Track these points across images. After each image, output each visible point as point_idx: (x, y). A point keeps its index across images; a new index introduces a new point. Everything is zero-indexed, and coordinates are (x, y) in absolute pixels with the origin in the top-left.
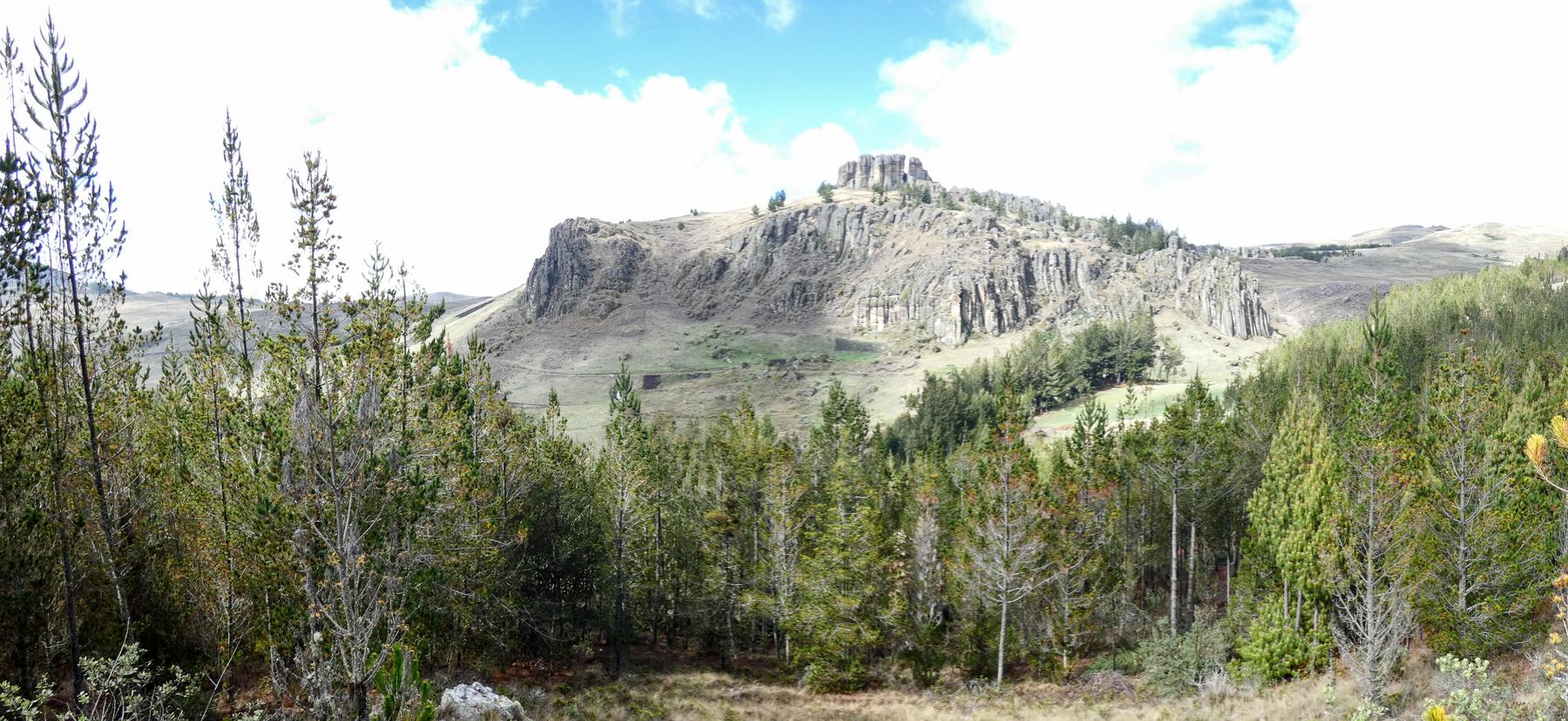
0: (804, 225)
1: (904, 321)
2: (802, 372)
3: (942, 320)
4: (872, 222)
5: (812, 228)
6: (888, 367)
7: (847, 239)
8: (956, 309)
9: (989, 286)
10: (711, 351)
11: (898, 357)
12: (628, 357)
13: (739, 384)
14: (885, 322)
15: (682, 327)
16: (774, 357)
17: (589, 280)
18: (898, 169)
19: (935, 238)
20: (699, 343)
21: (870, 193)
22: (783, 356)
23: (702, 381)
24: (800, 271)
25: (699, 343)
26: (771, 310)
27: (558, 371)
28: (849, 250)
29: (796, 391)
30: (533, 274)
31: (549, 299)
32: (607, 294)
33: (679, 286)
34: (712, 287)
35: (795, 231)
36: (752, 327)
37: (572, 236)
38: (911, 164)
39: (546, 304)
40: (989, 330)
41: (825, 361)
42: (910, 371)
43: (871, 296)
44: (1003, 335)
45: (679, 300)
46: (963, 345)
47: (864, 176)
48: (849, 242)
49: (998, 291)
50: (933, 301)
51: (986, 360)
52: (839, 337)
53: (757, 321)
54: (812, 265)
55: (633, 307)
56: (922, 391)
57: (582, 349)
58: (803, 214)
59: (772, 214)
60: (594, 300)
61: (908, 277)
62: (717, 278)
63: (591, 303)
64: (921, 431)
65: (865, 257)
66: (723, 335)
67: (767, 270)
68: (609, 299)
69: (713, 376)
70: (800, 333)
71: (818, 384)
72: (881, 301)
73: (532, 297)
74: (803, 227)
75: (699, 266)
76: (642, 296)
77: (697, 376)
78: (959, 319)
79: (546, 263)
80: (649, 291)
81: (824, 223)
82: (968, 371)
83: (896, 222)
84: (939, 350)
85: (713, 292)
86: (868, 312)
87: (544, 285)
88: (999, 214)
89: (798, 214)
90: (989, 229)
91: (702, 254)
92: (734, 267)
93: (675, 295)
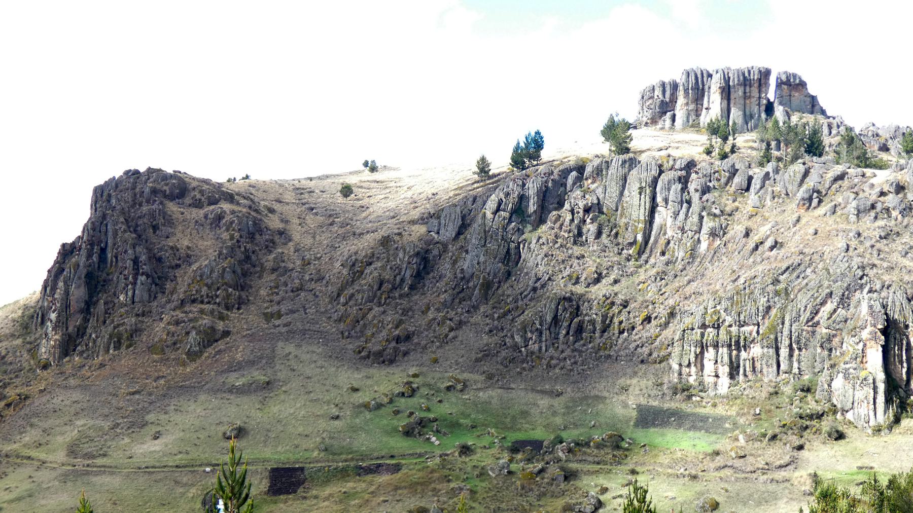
0: (578, 193)
1: (769, 374)
2: (573, 466)
3: (846, 377)
4: (706, 190)
5: (591, 199)
6: (738, 463)
7: (658, 220)
8: (875, 357)
10: (402, 422)
11: (757, 444)
12: (240, 433)
13: (452, 485)
14: (733, 375)
15: (347, 376)
16: (521, 436)
17: (169, 286)
18: (755, 93)
19: (831, 220)
20: (379, 406)
21: (703, 139)
22: (538, 434)
23: (384, 478)
25: (379, 406)
26: (516, 347)
27: (100, 461)
28: (662, 241)
30: (56, 273)
31: (86, 320)
32: (202, 312)
33: (342, 300)
34: (405, 302)
35: (561, 205)
36: (477, 378)
37: (136, 203)
38: (780, 84)
39: (81, 332)
41: (618, 447)
42: (781, 474)
43: (704, 326)
45: (342, 326)
46: (890, 428)
47: (692, 107)
48: (662, 228)
50: (829, 339)
52: (643, 401)
53: (486, 367)
54: (591, 266)
55: (252, 338)
57: (151, 417)
58: (574, 174)
59: (517, 173)
60: (177, 323)
61: (777, 293)
62: (412, 287)
63: (172, 328)
65: (693, 253)
66: (424, 391)
67: (509, 274)
68: (206, 321)
69: (404, 471)
70: (569, 392)
71: (604, 490)
73: (53, 316)
74: (576, 199)
75: (379, 264)
76: (268, 317)
77: (376, 469)
78: (881, 376)
79: (84, 252)
80: (283, 308)
81: (613, 190)
82: (903, 483)
83: (752, 189)
84: (840, 436)
85: (405, 312)
86: (700, 357)
87: (78, 293)
89: (566, 173)
91: (386, 241)
92: (445, 267)
93: (335, 316)
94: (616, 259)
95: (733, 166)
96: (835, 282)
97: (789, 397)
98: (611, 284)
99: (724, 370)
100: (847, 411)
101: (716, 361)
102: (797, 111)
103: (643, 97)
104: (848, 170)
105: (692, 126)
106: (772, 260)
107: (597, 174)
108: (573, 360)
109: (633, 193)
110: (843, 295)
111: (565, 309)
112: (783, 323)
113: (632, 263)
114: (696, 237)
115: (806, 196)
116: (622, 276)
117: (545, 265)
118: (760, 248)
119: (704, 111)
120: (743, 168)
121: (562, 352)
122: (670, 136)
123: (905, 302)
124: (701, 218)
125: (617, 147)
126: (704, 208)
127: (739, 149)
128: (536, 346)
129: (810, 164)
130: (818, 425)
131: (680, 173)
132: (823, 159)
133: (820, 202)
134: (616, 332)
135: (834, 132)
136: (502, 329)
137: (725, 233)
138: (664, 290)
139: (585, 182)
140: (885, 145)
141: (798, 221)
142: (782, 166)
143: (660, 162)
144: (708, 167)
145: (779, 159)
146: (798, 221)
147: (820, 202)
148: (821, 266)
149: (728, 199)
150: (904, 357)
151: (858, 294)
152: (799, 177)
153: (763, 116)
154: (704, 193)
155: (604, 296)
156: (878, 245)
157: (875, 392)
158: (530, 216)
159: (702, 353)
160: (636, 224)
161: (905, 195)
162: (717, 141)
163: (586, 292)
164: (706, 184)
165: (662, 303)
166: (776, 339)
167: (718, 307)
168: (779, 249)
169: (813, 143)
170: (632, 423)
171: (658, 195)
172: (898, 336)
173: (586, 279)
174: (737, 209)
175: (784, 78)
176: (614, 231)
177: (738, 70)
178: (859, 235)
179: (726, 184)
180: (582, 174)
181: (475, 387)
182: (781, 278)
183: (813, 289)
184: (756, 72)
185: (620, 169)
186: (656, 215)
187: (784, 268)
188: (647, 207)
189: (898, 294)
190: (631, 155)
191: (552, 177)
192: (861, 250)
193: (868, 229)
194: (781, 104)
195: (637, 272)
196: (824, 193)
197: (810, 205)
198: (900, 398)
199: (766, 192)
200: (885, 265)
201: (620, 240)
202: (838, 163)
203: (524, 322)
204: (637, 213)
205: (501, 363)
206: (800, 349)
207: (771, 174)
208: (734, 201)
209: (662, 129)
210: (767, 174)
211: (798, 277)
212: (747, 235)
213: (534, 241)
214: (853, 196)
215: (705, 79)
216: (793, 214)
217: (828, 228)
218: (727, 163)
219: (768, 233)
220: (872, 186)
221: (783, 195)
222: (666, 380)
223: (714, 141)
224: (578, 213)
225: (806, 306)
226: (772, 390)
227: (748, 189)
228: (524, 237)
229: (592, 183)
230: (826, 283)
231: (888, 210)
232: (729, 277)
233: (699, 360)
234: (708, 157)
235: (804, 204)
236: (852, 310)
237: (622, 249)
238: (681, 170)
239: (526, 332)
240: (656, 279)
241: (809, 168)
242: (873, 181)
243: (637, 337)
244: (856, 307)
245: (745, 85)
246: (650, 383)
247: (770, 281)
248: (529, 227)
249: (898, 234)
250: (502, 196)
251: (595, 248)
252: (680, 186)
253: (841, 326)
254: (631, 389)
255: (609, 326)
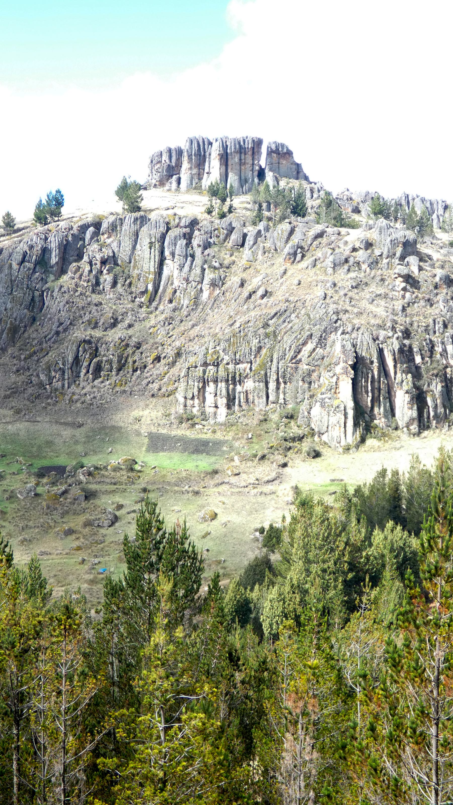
0: (95, 246)
1: (260, 404)
2: (93, 487)
3: (323, 406)
4: (207, 246)
5: (107, 252)
6: (233, 480)
7: (166, 272)
9: (401, 351)
11: (250, 464)
14: (229, 406)
16: (46, 463)
18: (249, 160)
19: (311, 272)
21: (205, 200)
22: (62, 461)
24: (89, 322)
26: (41, 385)
28: (170, 290)
29: (82, 519)
35: (80, 257)
38: (270, 152)
40: (401, 424)
44: (426, 433)
46: (357, 447)
48: (170, 279)
49: (418, 359)
50: (309, 374)
51: (395, 473)
52: (154, 430)
53: (14, 402)
56: (288, 520)
58: (92, 229)
59: (40, 228)
61: (267, 335)
64: (287, 588)
70: (90, 423)
71: (120, 507)
72: (222, 373)
78: (351, 404)
81: (127, 244)
82: (367, 492)
83: (246, 245)
84: (317, 455)
86: (202, 390)
88: (421, 233)
89: (84, 228)
90: (402, 258)
94: (129, 306)
95: (230, 224)
96: (315, 325)
97: (276, 423)
98: (126, 329)
99: (222, 402)
100: (323, 434)
101: (216, 394)
102: (284, 177)
103: (152, 162)
104: (326, 229)
105: (195, 188)
106: (263, 306)
107: (113, 230)
108: (92, 396)
109: (144, 248)
110: (321, 337)
111: (85, 351)
112: (272, 361)
113: (144, 309)
114: (199, 287)
115: (292, 251)
116: (135, 321)
117: (67, 311)
118: (253, 297)
119: (205, 175)
120: (239, 226)
121: (83, 388)
122: (176, 197)
123: (371, 341)
124: (203, 270)
125: (130, 206)
126: (206, 262)
127: (235, 209)
128: (60, 383)
129: (295, 223)
130: (299, 446)
131: (184, 230)
132: (306, 219)
133: (303, 256)
134: (131, 370)
135: (315, 195)
136: (28, 369)
137: (223, 284)
138: (171, 333)
139: (102, 237)
140: (357, 208)
141: (285, 273)
142: (272, 225)
143: (167, 220)
144: (209, 225)
145: (269, 219)
146: (285, 273)
147: (303, 256)
148: (303, 312)
149: (226, 254)
150: (370, 388)
151: (333, 336)
152: (286, 234)
153: (256, 180)
154: (205, 248)
155: (120, 338)
156: (350, 294)
157: (346, 418)
158: (52, 267)
159: (204, 387)
160: (147, 275)
161: (373, 250)
162: (216, 202)
163: (104, 335)
164: (207, 240)
165: (170, 345)
166: (266, 374)
167: (218, 348)
168: (269, 298)
169: (298, 205)
170: (144, 449)
171: (166, 249)
172: (364, 370)
173: (103, 324)
174: (234, 262)
175: (273, 147)
176: (128, 281)
177: (235, 140)
178: (335, 285)
179: (225, 241)
180: (99, 229)
181: (4, 421)
182: (271, 322)
183: (296, 332)
184: (250, 142)
185: (132, 225)
186: (165, 267)
187: (273, 314)
188: (157, 260)
189: (365, 335)
190: (142, 213)
191: (72, 232)
192: (336, 298)
193: (343, 280)
194: (271, 170)
195: (148, 318)
196: (306, 248)
197: (295, 259)
198: (366, 422)
199: (258, 248)
200: (356, 310)
201: (133, 289)
202: (318, 223)
203: (48, 362)
204: (148, 265)
205: (28, 399)
206: (285, 383)
207: (263, 232)
208: (231, 256)
209: (169, 190)
210: (259, 231)
211: (284, 321)
212: (242, 285)
213: (57, 290)
214: (330, 251)
215: (206, 147)
216: (281, 267)
217: (309, 279)
218: (225, 222)
219: (260, 283)
220: (346, 243)
221: (272, 251)
222: (173, 411)
223: (214, 202)
224: (96, 264)
225: (291, 346)
226: (262, 418)
227: (243, 245)
228: (47, 286)
229: (108, 238)
230: (307, 327)
231: (358, 263)
232: (227, 322)
233: (201, 393)
234: (209, 216)
235: (290, 259)
236: (328, 349)
237: (135, 298)
238: (186, 227)
239: (50, 371)
240: (164, 323)
241: (294, 227)
242: (346, 238)
243: (148, 374)
244: (331, 347)
245: (241, 153)
246: (160, 414)
247: (261, 325)
248: (52, 277)
249: (366, 284)
250: (26, 248)
251: (111, 296)
252: (185, 242)
253: (319, 363)
254: (143, 420)
255: (124, 365)
